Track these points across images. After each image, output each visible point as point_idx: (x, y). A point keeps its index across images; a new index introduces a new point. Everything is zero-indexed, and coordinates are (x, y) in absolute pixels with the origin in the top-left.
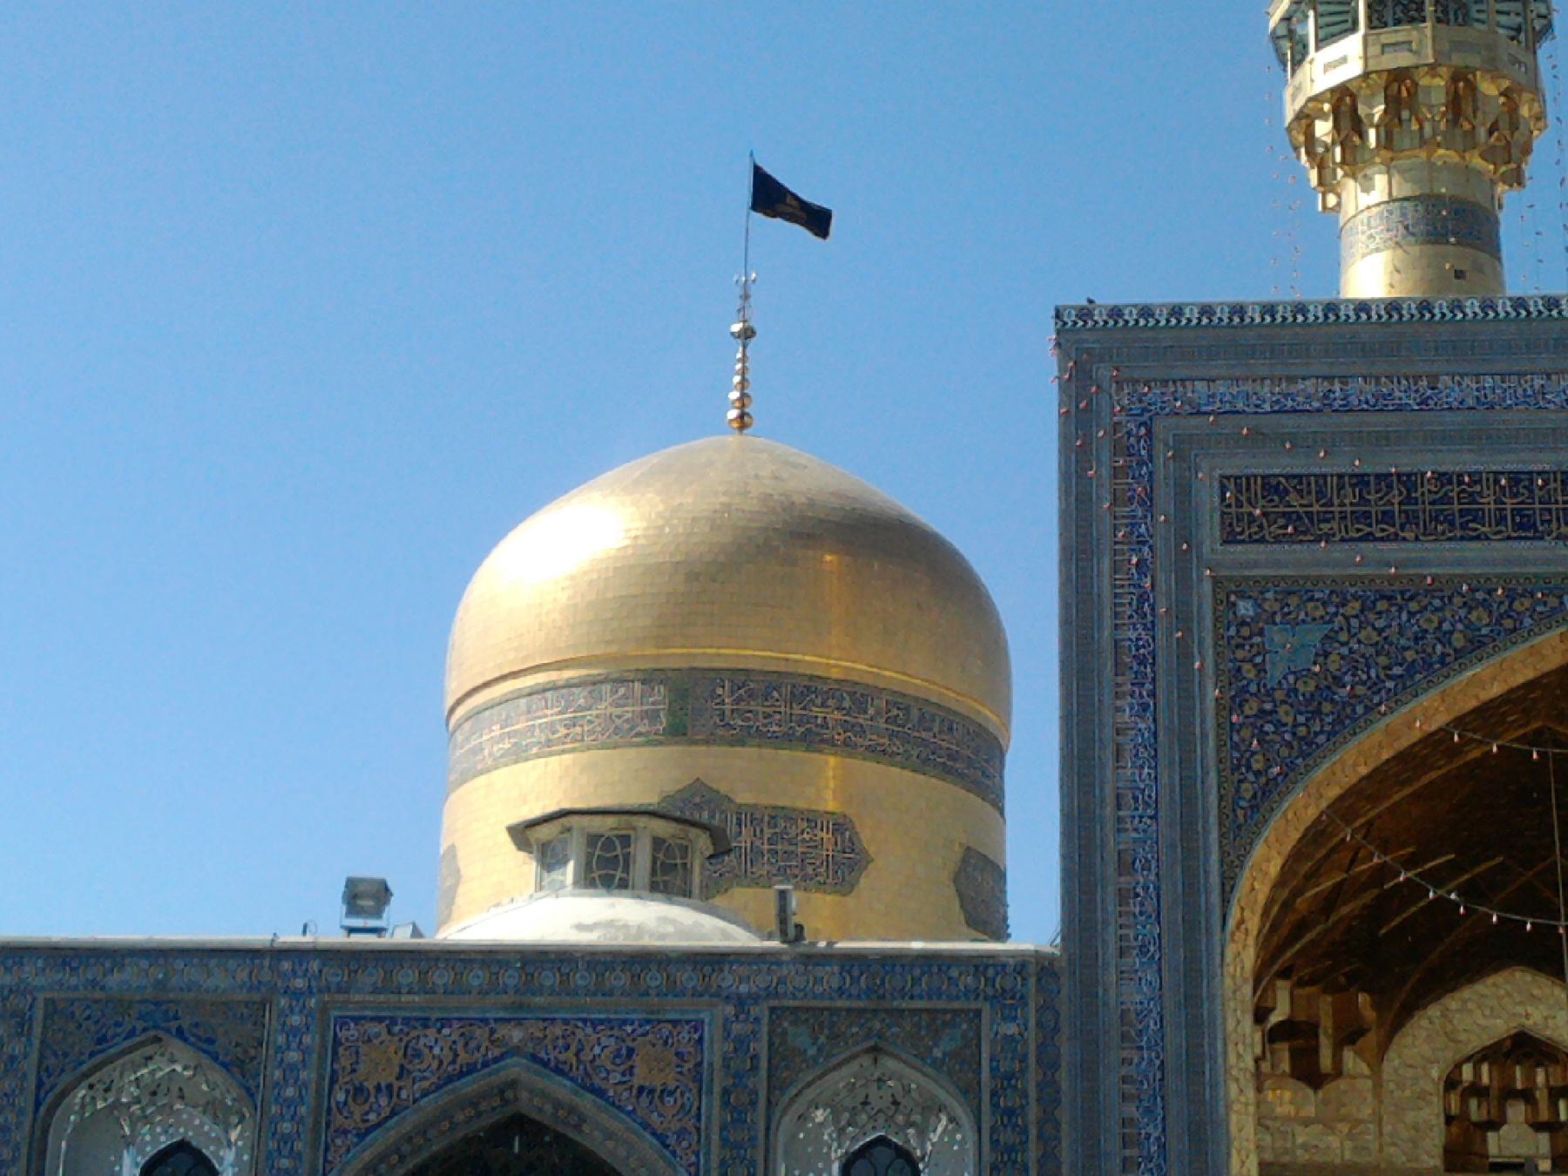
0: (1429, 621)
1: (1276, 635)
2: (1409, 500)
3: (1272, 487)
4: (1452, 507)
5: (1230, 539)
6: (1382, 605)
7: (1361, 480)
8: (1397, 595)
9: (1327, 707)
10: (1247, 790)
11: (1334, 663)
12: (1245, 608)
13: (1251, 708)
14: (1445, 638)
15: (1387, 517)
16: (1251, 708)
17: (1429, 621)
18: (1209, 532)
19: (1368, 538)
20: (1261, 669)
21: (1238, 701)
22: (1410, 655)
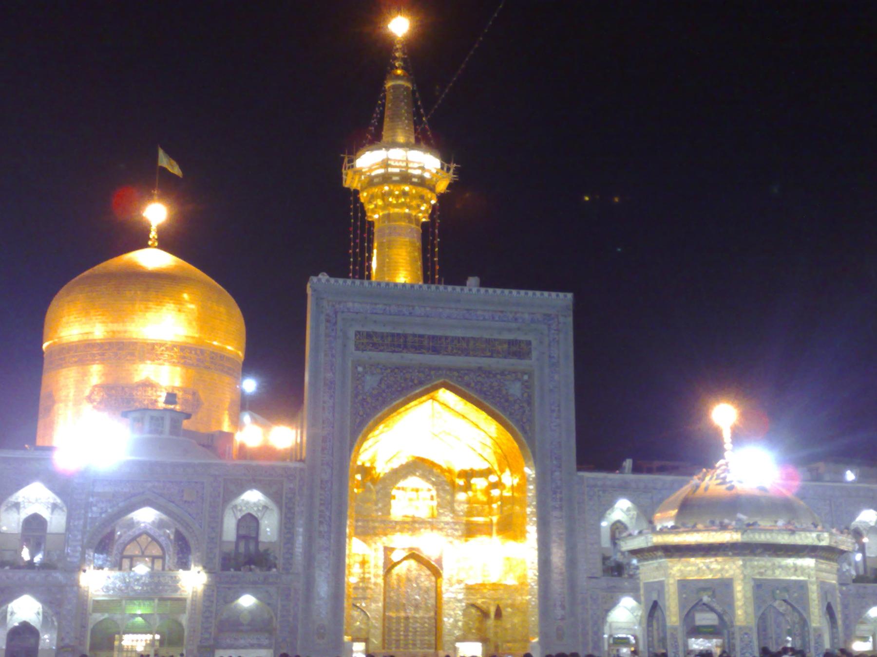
0: (408, 376)
1: (368, 378)
2: (405, 342)
3: (369, 335)
4: (418, 344)
5: (357, 349)
6: (396, 371)
7: (393, 335)
8: (400, 368)
9: (380, 398)
10: (358, 420)
11: (383, 386)
12: (360, 369)
13: (360, 397)
14: (412, 381)
15: (399, 346)
16: (360, 397)
17: (408, 376)
18: (351, 345)
19: (394, 352)
20: (363, 387)
21: (356, 396)
22: (403, 385)
